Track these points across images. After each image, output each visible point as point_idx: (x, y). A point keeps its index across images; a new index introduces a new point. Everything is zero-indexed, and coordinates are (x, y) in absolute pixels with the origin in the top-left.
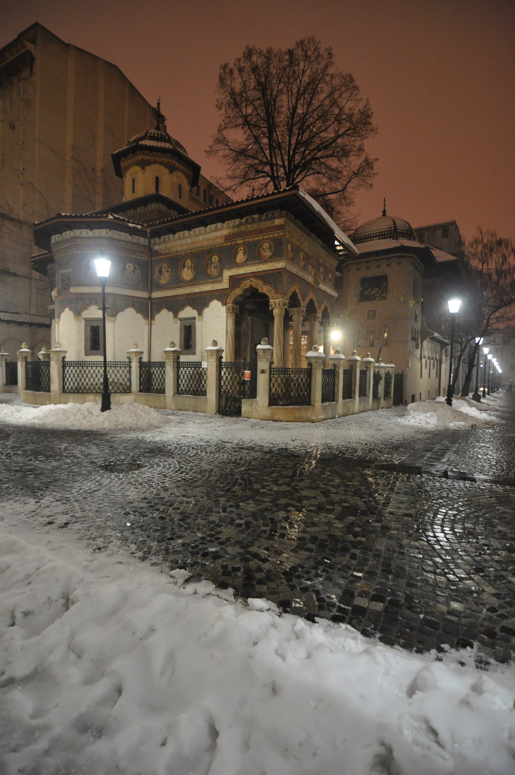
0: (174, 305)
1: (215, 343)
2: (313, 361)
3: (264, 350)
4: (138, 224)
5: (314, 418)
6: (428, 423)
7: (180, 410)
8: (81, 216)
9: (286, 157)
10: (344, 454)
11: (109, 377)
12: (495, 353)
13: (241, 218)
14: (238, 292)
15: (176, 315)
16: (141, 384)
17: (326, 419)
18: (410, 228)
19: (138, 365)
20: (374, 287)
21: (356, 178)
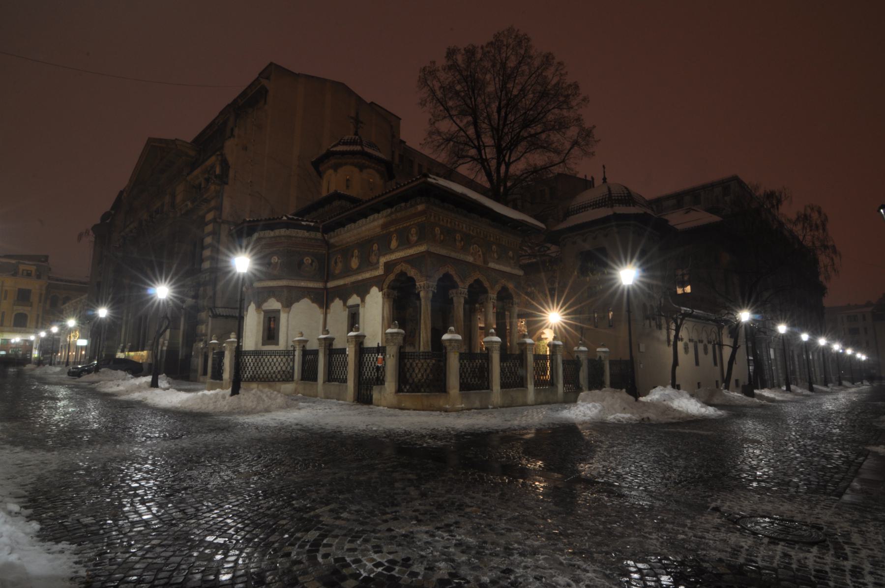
0: (343, 294)
2: (447, 344)
3: (392, 334)
7: (328, 398)
13: (392, 207)
14: (392, 277)
16: (303, 371)
18: (629, 193)
21: (576, 148)
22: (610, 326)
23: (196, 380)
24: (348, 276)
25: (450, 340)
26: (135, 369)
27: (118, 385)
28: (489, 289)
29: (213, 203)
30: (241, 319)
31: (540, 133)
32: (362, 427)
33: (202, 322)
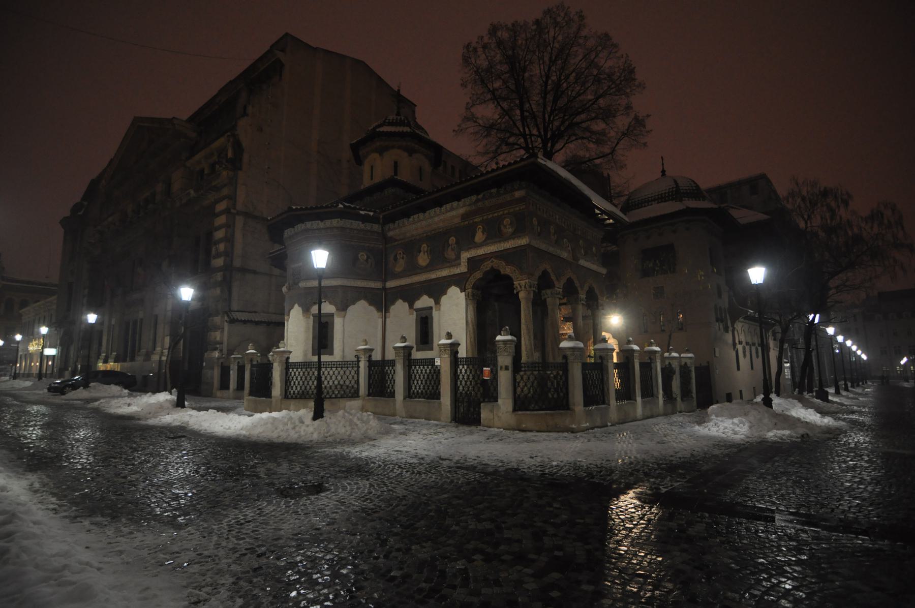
0: (409, 295)
1: (449, 336)
2: (568, 353)
3: (505, 342)
4: (370, 211)
6: (736, 433)
7: (411, 417)
8: (322, 207)
9: (541, 126)
10: (593, 478)
11: (323, 379)
12: (847, 335)
13: (478, 194)
14: (478, 275)
15: (411, 306)
16: (370, 386)
17: (592, 428)
18: (697, 186)
19: (367, 364)
20: (660, 259)
22: (681, 329)
23: (209, 395)
25: (573, 349)
26: (136, 384)
27: (129, 405)
28: (579, 289)
29: (225, 191)
33: (216, 328)
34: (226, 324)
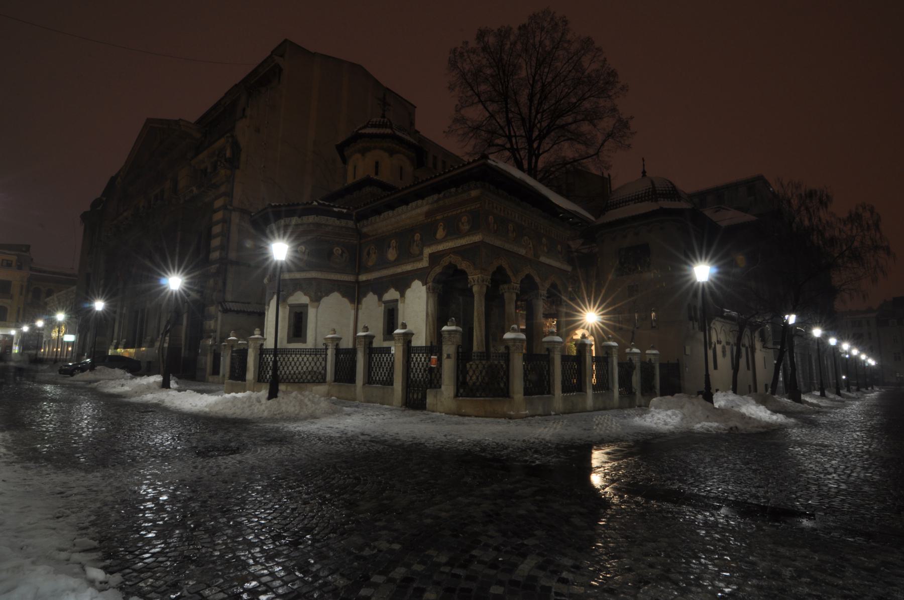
2: (510, 344)
3: (449, 331)
4: (344, 208)
5: (512, 413)
6: (666, 424)
7: (369, 402)
13: (439, 192)
14: (438, 270)
15: (380, 298)
17: (533, 416)
18: (674, 187)
22: (653, 327)
23: (203, 380)
24: (385, 268)
25: (514, 340)
26: (135, 368)
27: (123, 385)
29: (223, 189)
30: (262, 315)
31: (571, 124)
32: (440, 437)
34: (219, 314)
